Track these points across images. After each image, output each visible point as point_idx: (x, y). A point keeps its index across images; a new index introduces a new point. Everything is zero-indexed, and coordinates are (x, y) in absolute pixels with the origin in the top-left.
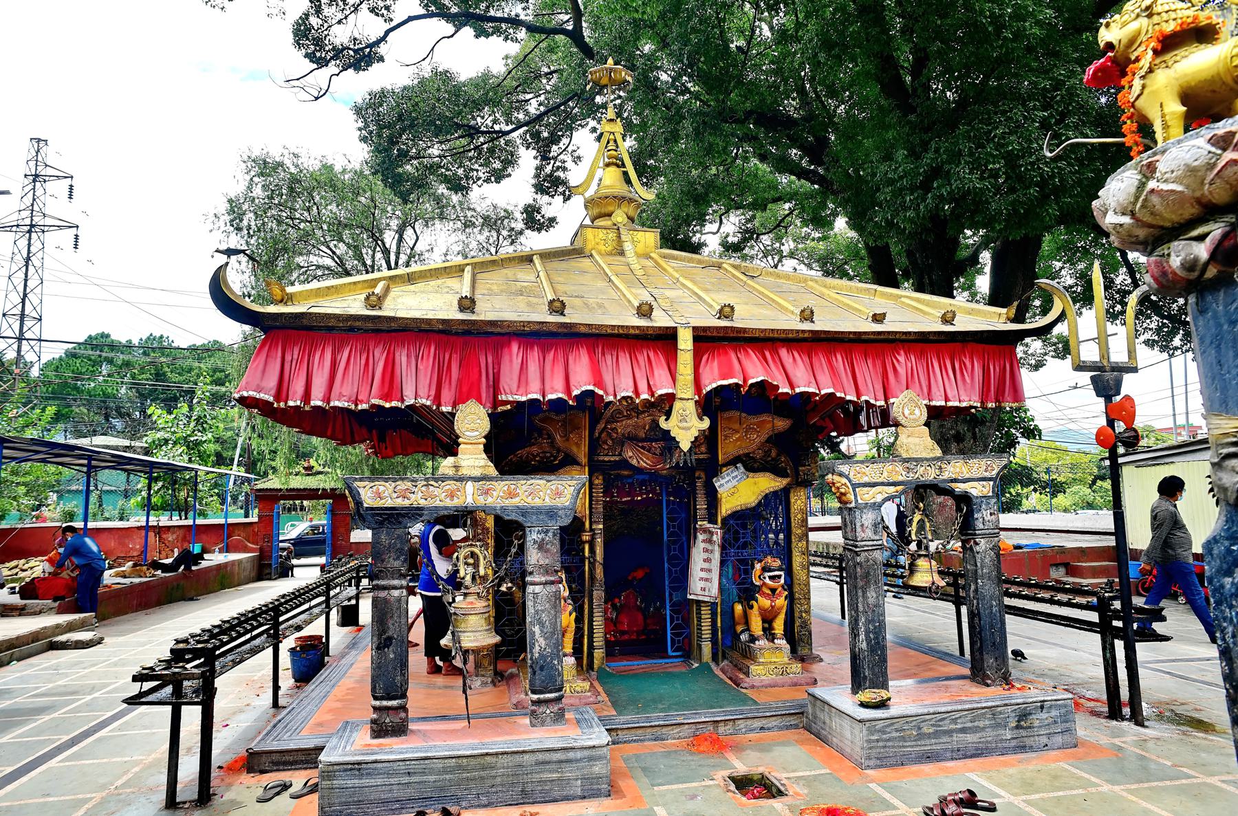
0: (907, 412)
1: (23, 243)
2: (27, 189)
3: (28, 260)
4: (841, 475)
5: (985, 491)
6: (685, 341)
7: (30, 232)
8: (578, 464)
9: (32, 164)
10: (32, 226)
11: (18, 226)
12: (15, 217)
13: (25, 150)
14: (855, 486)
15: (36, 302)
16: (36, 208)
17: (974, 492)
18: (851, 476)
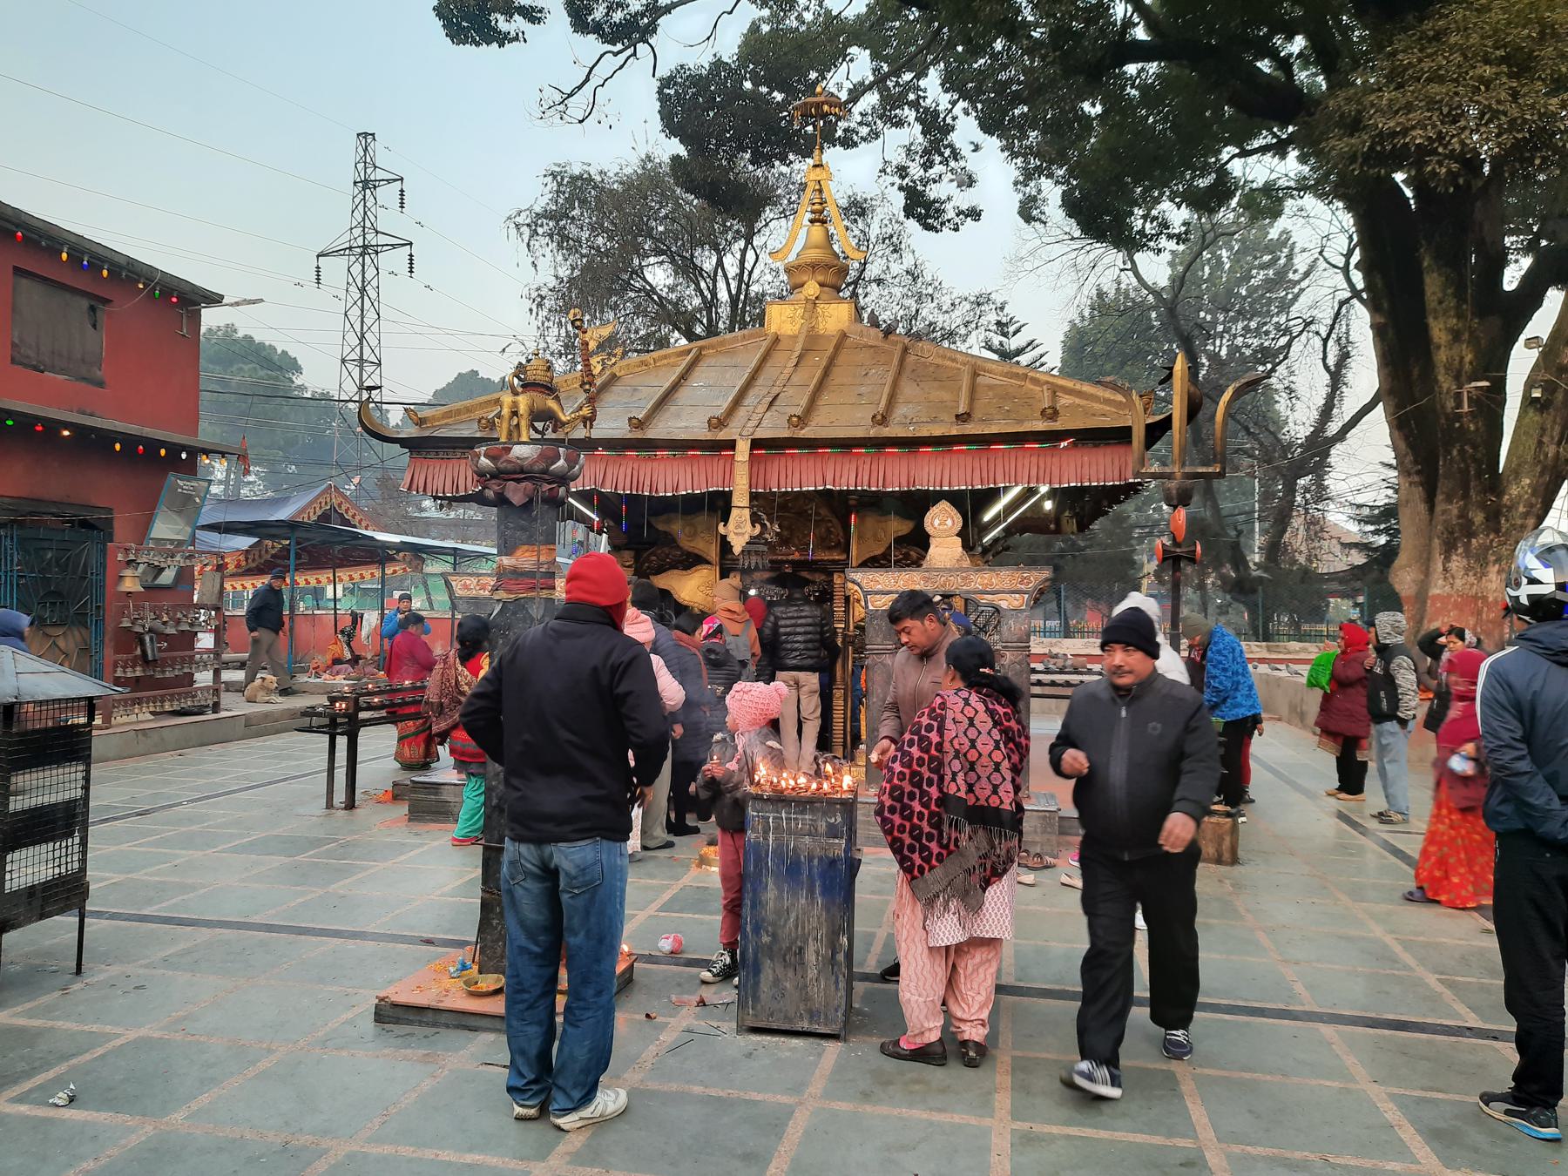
0: (936, 522)
1: (356, 269)
2: (357, 200)
3: (363, 291)
4: (853, 582)
5: (1016, 603)
6: (743, 451)
7: (362, 255)
8: (708, 563)
9: (361, 166)
10: (365, 247)
11: (350, 248)
12: (347, 237)
13: (349, 150)
14: (866, 593)
15: (374, 343)
16: (368, 224)
17: (1004, 604)
18: (864, 585)
